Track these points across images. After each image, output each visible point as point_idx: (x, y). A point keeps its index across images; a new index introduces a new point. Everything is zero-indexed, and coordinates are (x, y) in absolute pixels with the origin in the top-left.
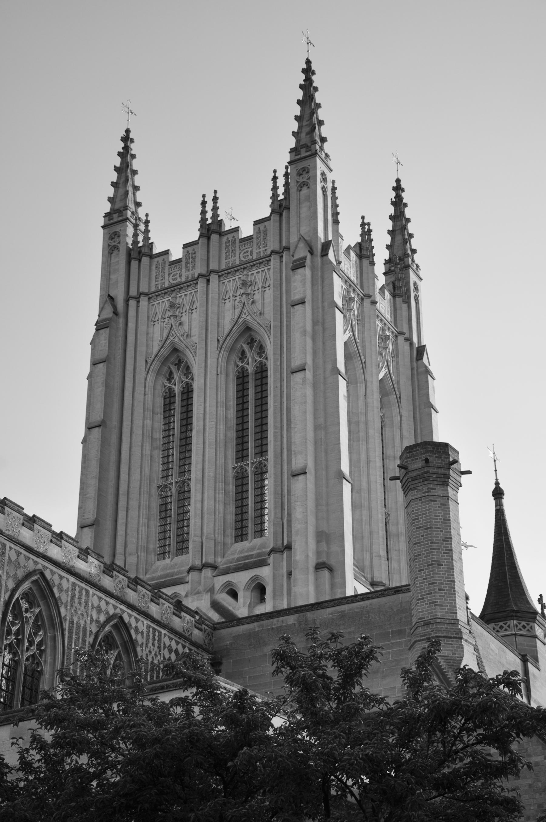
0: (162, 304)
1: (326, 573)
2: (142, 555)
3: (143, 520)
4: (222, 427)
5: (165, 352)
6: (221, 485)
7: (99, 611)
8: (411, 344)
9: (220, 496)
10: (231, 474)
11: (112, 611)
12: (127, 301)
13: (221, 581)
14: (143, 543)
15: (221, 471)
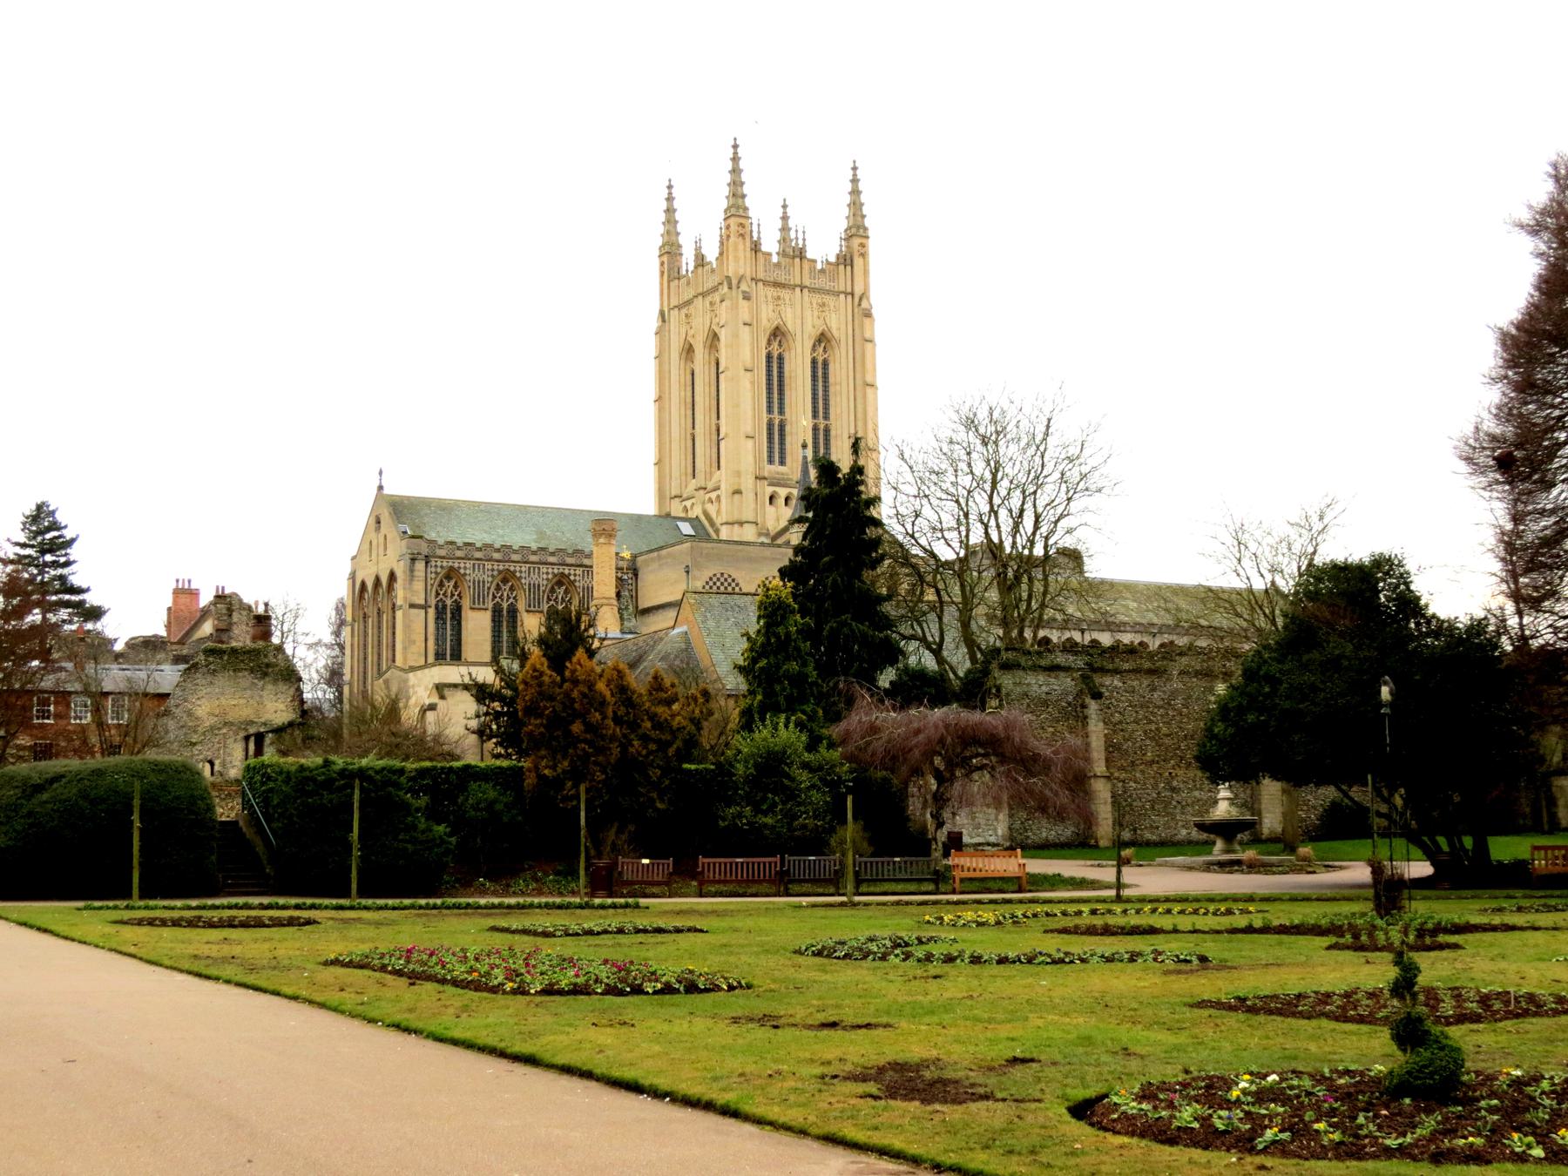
0: (684, 311)
1: (737, 496)
2: (683, 478)
3: (683, 457)
4: (707, 399)
5: (687, 346)
6: (707, 437)
7: (547, 573)
8: (852, 294)
9: (708, 443)
10: (714, 428)
11: (556, 571)
12: (669, 312)
13: (707, 496)
14: (683, 471)
15: (707, 428)
